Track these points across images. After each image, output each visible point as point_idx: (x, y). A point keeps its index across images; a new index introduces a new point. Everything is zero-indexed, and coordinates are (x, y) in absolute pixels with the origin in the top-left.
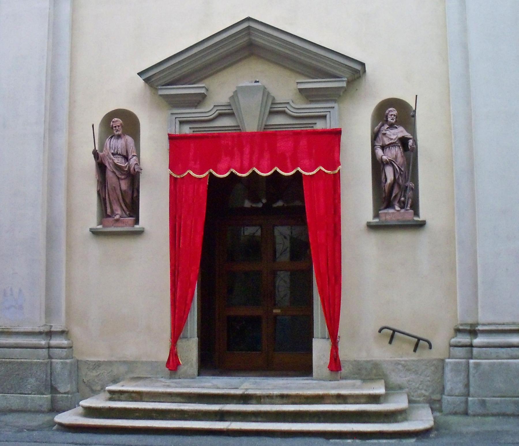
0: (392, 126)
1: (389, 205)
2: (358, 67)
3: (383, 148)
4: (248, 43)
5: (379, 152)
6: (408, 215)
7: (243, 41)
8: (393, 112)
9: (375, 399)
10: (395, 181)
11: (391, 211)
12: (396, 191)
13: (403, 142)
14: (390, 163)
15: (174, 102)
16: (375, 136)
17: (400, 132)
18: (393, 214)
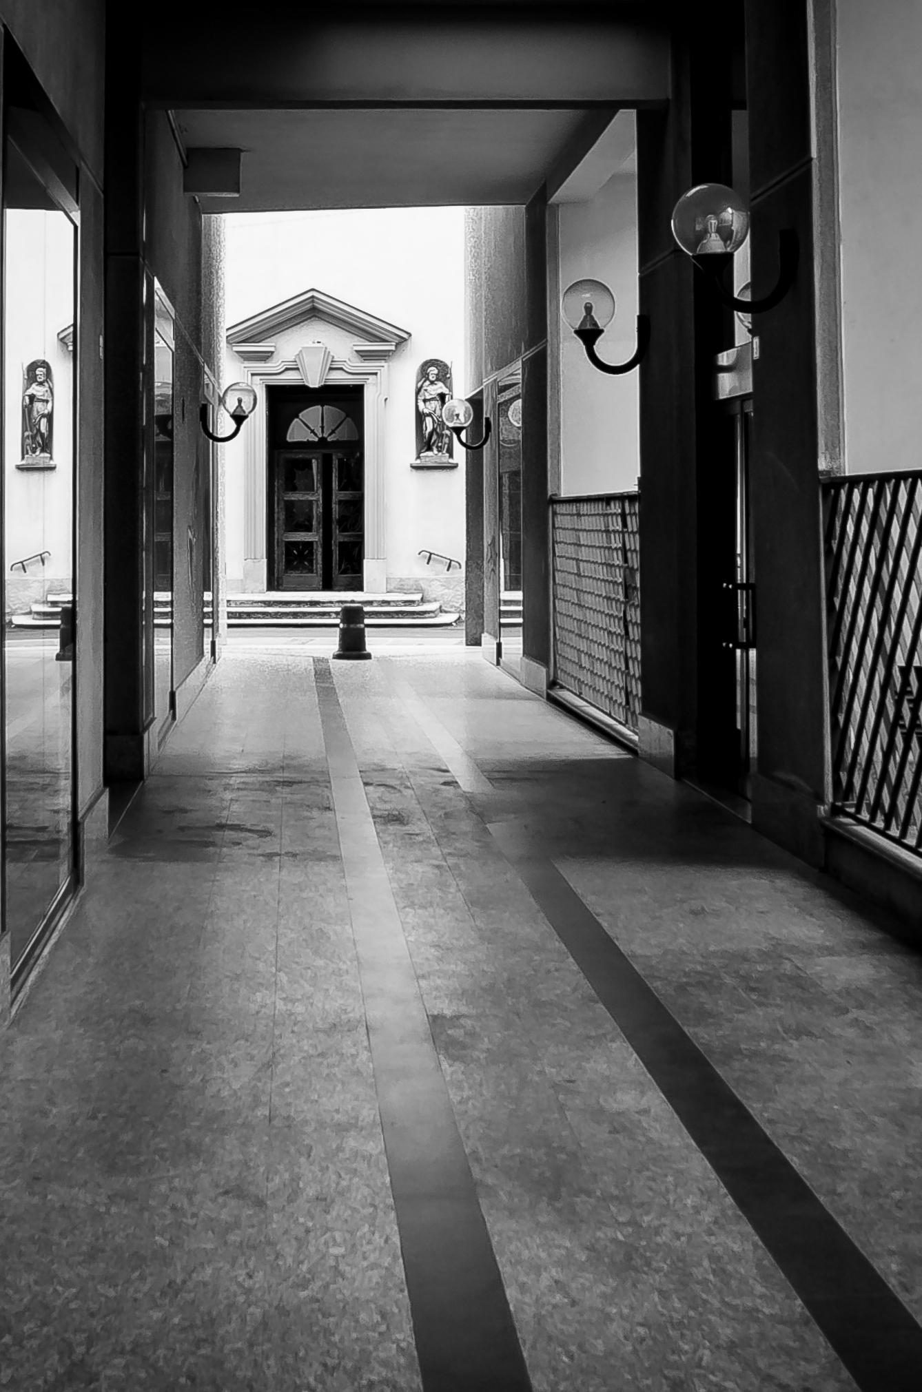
0: (432, 383)
1: (429, 449)
2: (405, 336)
3: (425, 401)
4: (310, 310)
5: (421, 405)
6: (444, 458)
7: (309, 306)
8: (433, 371)
9: (411, 602)
10: (434, 430)
11: (429, 453)
12: (434, 437)
13: (442, 397)
14: (429, 415)
15: (247, 357)
16: (418, 391)
17: (440, 388)
18: (431, 457)
